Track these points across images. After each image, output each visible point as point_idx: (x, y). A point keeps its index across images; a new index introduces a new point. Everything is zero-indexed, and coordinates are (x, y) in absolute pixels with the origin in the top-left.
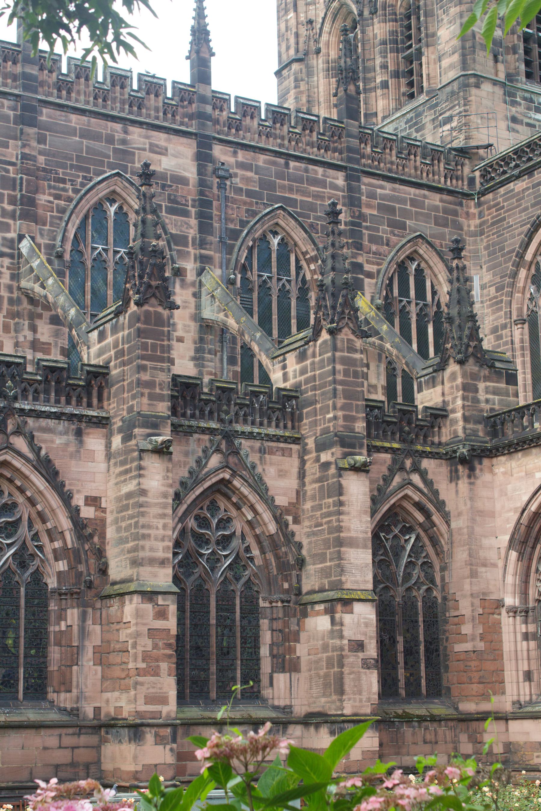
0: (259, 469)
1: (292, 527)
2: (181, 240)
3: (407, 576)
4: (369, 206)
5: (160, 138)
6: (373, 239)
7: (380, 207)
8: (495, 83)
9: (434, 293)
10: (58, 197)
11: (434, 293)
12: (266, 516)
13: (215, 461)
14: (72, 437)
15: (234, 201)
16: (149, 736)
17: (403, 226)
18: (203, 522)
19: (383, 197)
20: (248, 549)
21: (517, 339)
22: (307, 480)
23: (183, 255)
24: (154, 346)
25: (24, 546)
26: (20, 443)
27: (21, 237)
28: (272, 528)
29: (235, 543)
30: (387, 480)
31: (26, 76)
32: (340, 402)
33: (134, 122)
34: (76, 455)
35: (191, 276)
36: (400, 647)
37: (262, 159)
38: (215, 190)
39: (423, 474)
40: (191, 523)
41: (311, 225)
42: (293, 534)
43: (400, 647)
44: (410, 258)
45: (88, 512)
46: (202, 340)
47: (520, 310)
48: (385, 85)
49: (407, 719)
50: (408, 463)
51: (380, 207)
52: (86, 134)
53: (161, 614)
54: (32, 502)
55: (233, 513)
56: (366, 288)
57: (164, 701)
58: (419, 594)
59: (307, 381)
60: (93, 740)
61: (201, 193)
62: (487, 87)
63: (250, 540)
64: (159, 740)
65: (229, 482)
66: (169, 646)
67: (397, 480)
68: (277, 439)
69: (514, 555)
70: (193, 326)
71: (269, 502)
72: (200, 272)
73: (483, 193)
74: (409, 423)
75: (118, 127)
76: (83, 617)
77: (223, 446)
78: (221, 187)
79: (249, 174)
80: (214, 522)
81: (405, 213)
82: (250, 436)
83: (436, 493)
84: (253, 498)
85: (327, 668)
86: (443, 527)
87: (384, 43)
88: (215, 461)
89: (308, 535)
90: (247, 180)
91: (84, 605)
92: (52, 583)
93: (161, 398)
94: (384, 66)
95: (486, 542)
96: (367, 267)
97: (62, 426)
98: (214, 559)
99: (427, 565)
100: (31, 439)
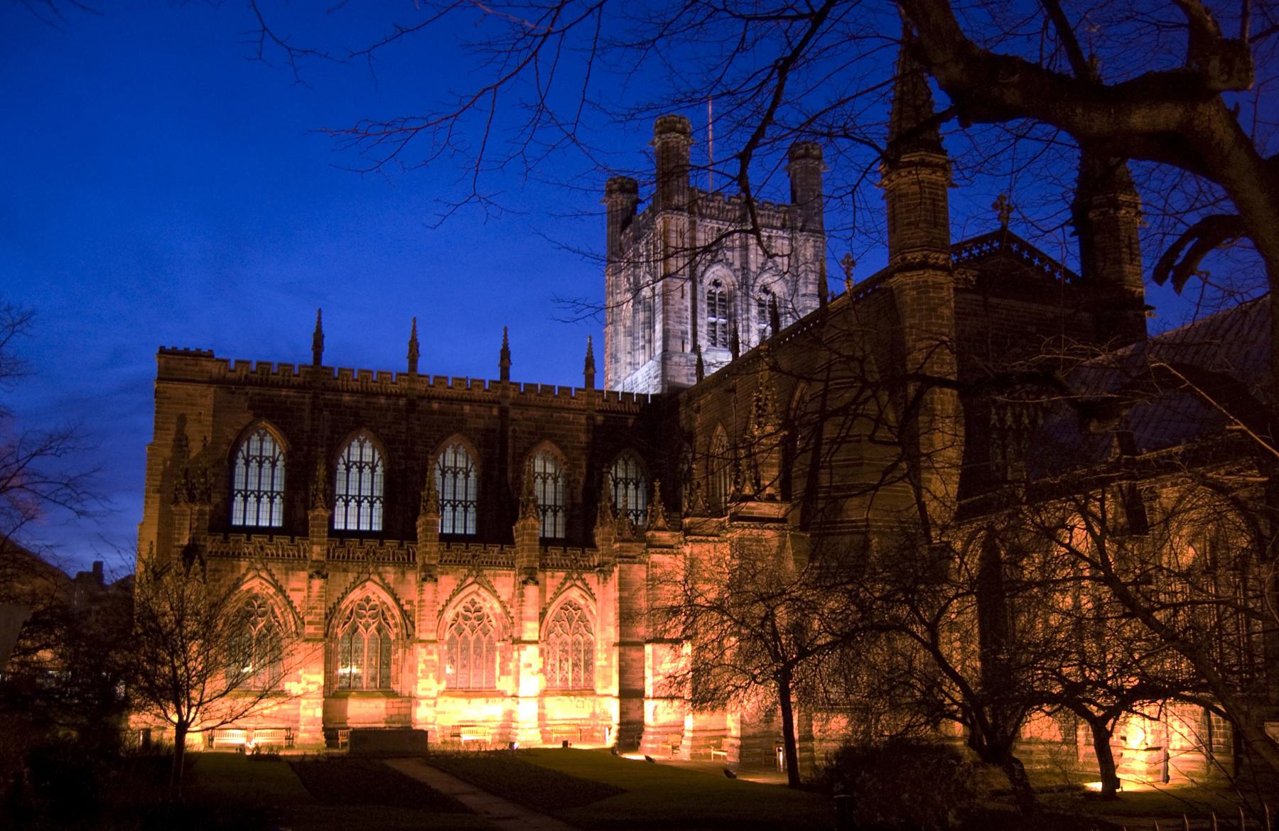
1: (509, 609)
12: (496, 605)
28: (498, 609)
30: (563, 584)
32: (525, 555)
34: (402, 582)
39: (583, 580)
40: (460, 609)
45: (406, 607)
48: (644, 347)
67: (568, 585)
86: (593, 607)
87: (644, 323)
94: (644, 337)
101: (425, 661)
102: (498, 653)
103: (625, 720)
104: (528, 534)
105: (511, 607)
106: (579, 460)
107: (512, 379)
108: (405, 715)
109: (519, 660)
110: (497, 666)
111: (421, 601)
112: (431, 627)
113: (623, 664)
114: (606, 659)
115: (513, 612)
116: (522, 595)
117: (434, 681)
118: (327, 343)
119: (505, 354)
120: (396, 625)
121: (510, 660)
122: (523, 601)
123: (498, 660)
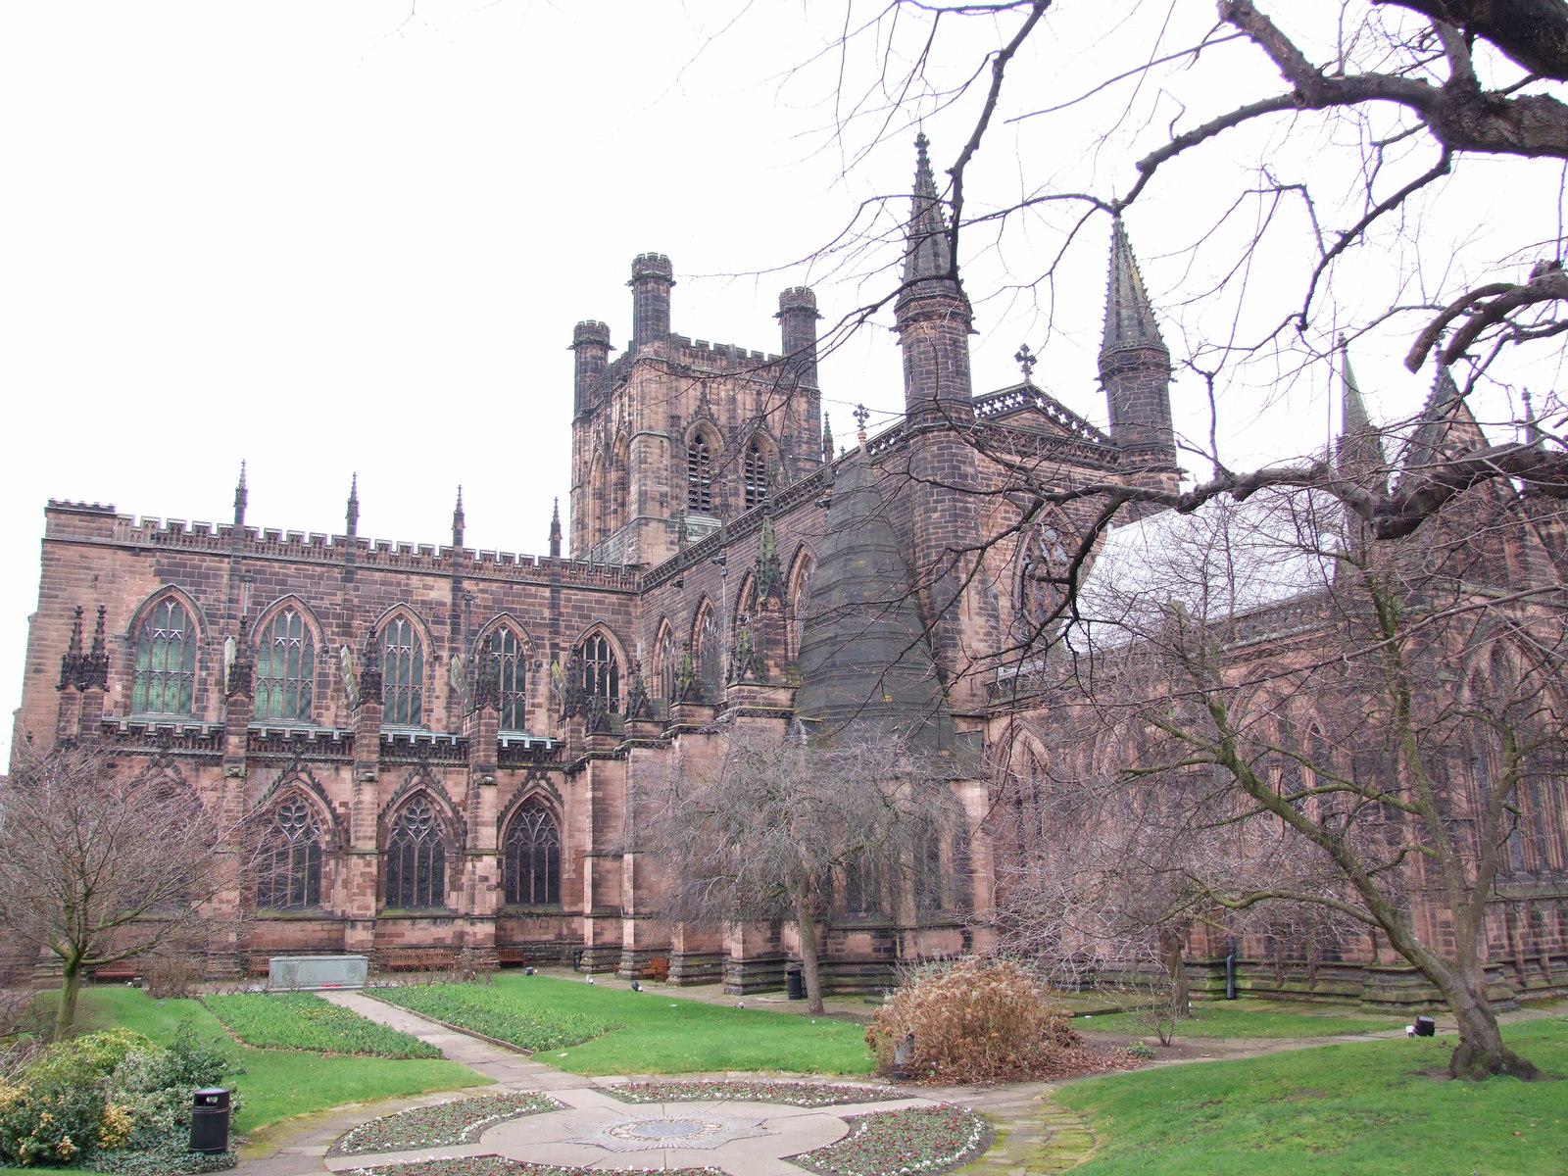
0: (443, 783)
2: (440, 639)
3: (539, 836)
4: (566, 607)
5: (430, 580)
6: (567, 627)
7: (574, 607)
8: (659, 521)
9: (612, 655)
10: (365, 621)
11: (612, 655)
12: (447, 808)
13: (416, 779)
14: (333, 772)
15: (475, 613)
16: (359, 925)
17: (589, 617)
18: (413, 812)
19: (576, 601)
20: (439, 825)
21: (655, 684)
23: (441, 648)
24: (371, 725)
25: (309, 828)
26: (304, 776)
27: (342, 646)
28: (450, 814)
29: (431, 822)
30: (524, 785)
31: (348, 554)
33: (413, 573)
35: (445, 660)
36: (533, 876)
37: (494, 586)
38: (463, 608)
39: (548, 780)
40: (404, 812)
41: (526, 623)
42: (462, 817)
43: (533, 876)
44: (596, 635)
45: (341, 810)
46: (450, 697)
47: (657, 667)
49: (530, 915)
50: (538, 774)
51: (574, 607)
52: (383, 583)
53: (369, 865)
54: (312, 805)
55: (430, 806)
56: (561, 656)
57: (368, 908)
58: (546, 847)
60: (341, 926)
61: (454, 610)
62: (653, 525)
63: (440, 821)
64: (365, 928)
65: (424, 791)
66: (372, 881)
67: (531, 784)
68: (455, 766)
70: (446, 689)
71: (449, 801)
72: (451, 657)
73: (644, 593)
74: (540, 751)
75: (404, 576)
76: (337, 865)
77: (421, 771)
78: (468, 605)
79: (486, 596)
80: (418, 812)
81: (591, 609)
82: (438, 765)
83: (556, 790)
84: (439, 799)
88: (416, 779)
90: (486, 599)
91: (338, 858)
92: (323, 846)
93: (374, 752)
95: (580, 818)
96: (562, 645)
97: (329, 765)
98: (418, 832)
99: (553, 831)
100: (310, 774)
101: (362, 874)
102: (447, 864)
103: (599, 942)
104: (486, 724)
105: (464, 810)
106: (543, 639)
107: (465, 545)
108: (337, 940)
109: (474, 873)
110: (446, 879)
111: (357, 803)
112: (369, 834)
113: (596, 875)
114: (574, 871)
115: (466, 816)
116: (477, 796)
117: (373, 899)
118: (250, 498)
119: (459, 516)
120: (326, 833)
121: (462, 872)
122: (478, 803)
123: (448, 872)
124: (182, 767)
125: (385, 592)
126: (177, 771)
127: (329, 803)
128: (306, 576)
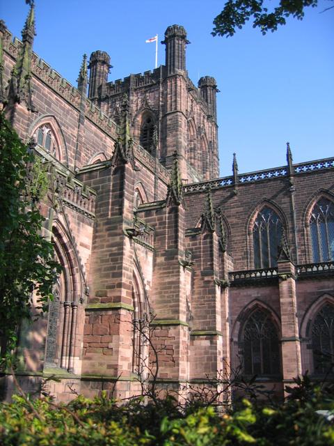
7: (161, 191)
22: (195, 286)
59: (196, 249)
69: (238, 323)
85: (207, 360)
89: (195, 308)
124: (70, 219)
125: (96, 141)
126: (65, 217)
127: (143, 280)
128: (61, 107)
